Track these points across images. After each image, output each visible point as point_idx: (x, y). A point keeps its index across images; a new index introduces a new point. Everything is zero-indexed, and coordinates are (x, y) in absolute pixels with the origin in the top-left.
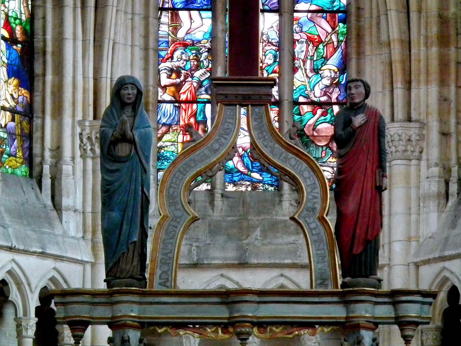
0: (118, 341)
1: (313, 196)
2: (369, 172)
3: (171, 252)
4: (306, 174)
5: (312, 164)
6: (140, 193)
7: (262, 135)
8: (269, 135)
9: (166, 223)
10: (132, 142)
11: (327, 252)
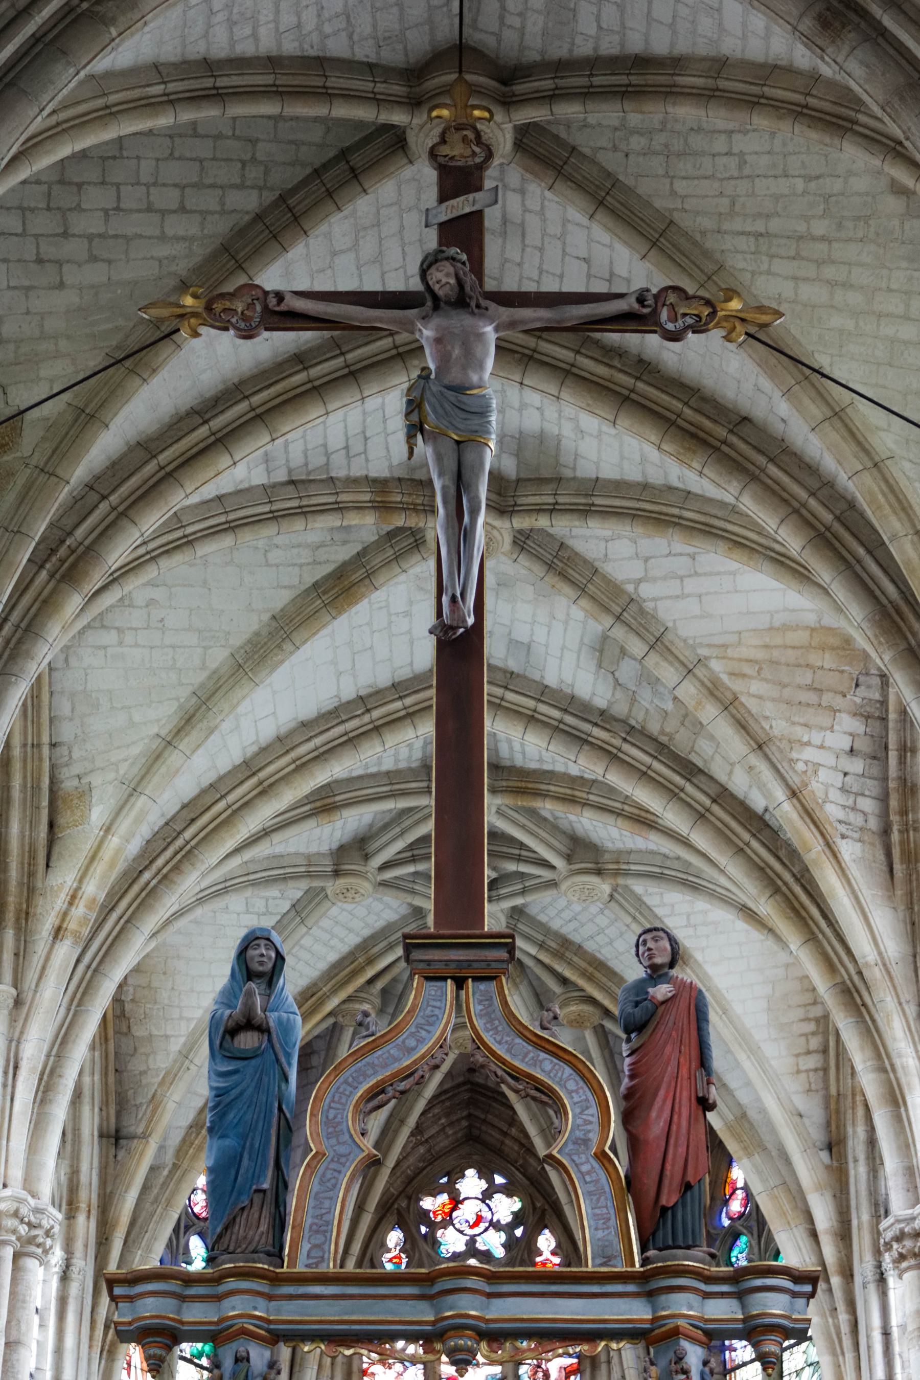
0: (228, 1364)
1: (585, 1120)
2: (684, 1072)
3: (329, 1212)
4: (571, 1085)
5: (580, 1066)
6: (276, 1111)
7: (492, 1024)
8: (505, 1025)
9: (321, 1168)
10: (263, 1029)
11: (612, 1212)
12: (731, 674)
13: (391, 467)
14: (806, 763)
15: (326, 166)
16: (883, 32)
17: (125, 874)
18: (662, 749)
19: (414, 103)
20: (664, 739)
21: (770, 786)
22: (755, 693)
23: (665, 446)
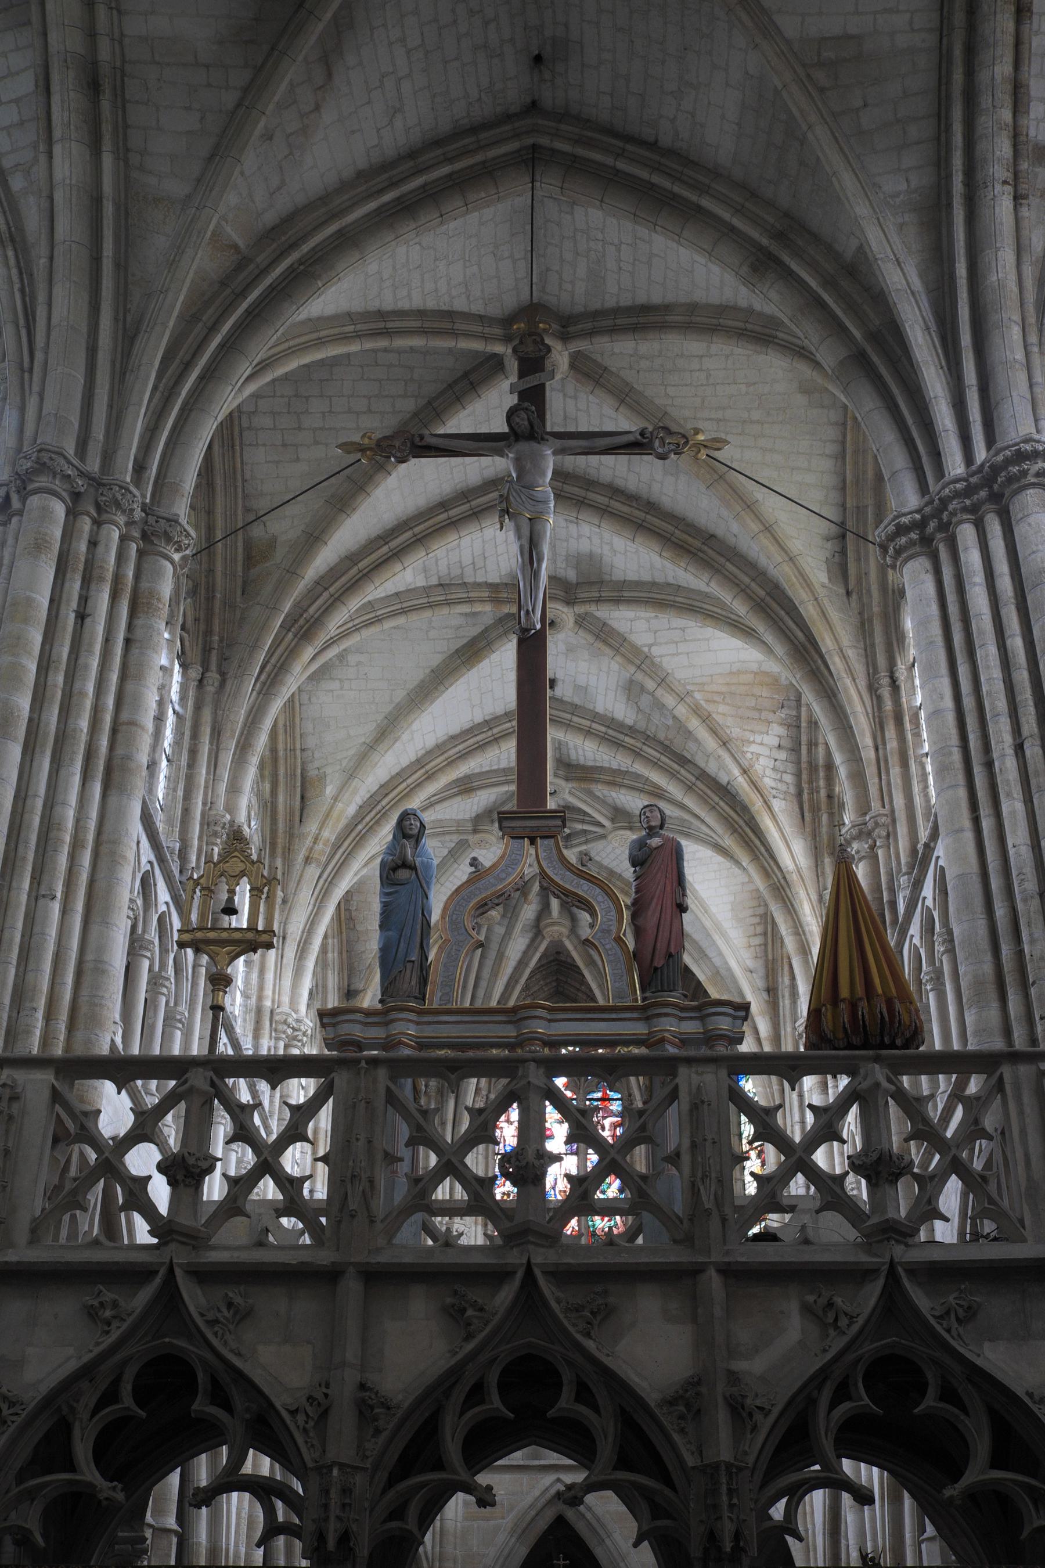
2: (668, 889)
4: (600, 898)
10: (413, 868)
12: (707, 701)
13: (500, 576)
14: (752, 753)
15: (456, 382)
16: (791, 273)
17: (347, 826)
18: (666, 748)
20: (667, 743)
21: (730, 767)
22: (721, 713)
23: (664, 554)
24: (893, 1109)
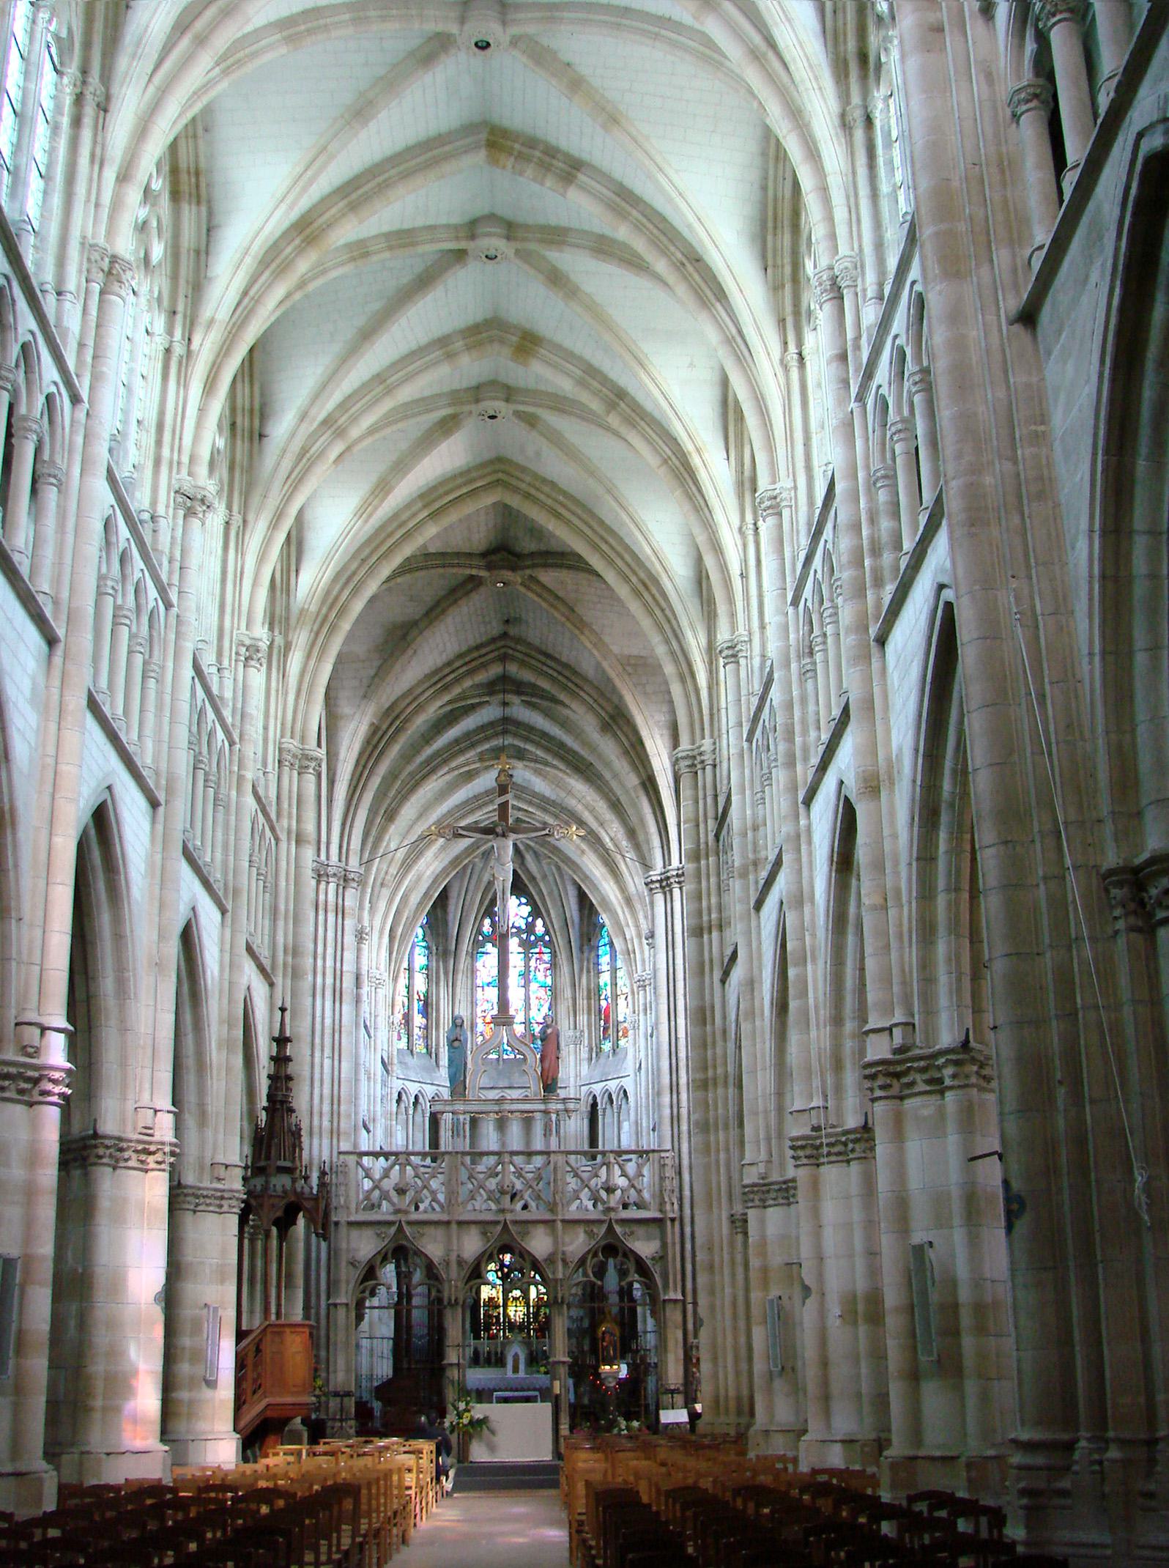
19: (491, 693)
24: (616, 1167)
